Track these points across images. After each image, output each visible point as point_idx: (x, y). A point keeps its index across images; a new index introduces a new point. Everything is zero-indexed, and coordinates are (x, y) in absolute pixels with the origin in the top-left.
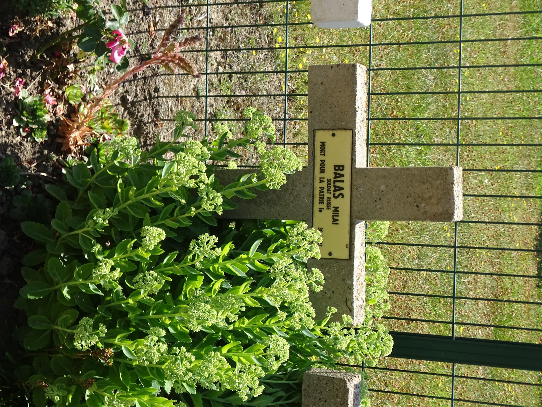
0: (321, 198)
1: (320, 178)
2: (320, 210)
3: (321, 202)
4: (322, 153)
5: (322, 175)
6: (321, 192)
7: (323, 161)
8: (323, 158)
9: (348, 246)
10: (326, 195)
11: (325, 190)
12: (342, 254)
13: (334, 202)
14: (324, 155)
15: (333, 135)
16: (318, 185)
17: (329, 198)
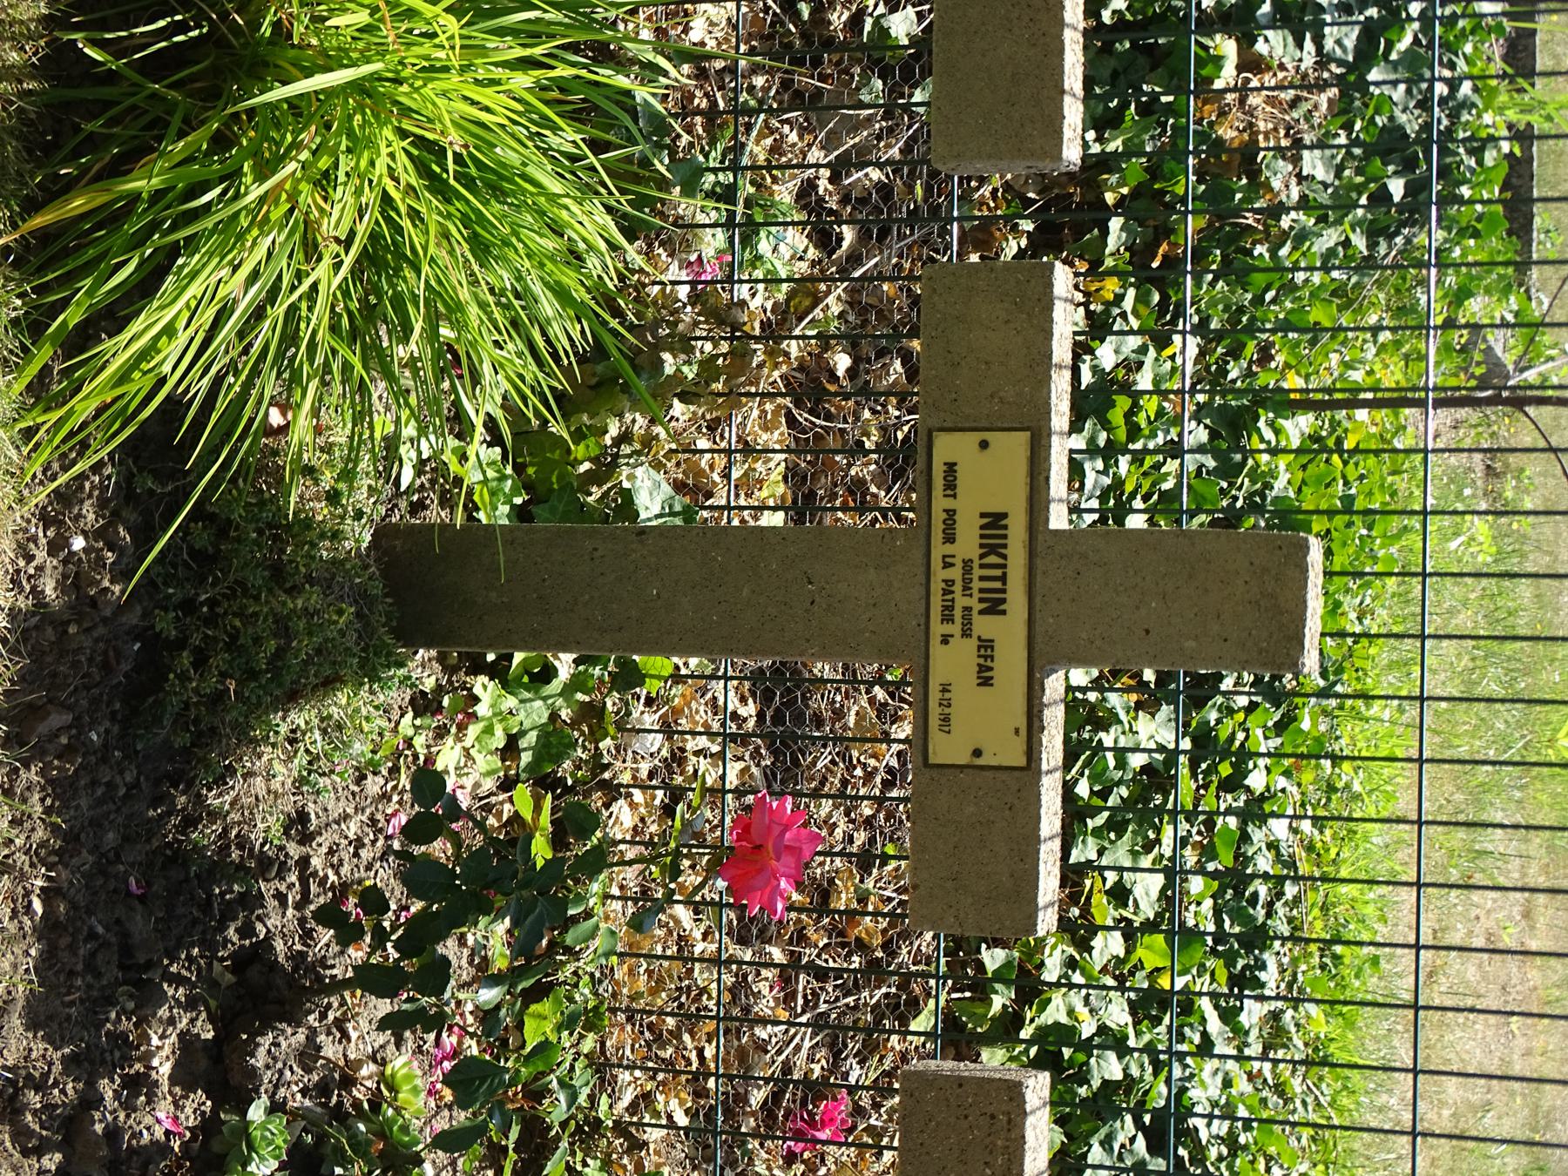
0: (945, 608)
2: (945, 640)
3: (948, 618)
5: (949, 549)
6: (946, 592)
7: (951, 513)
8: (949, 503)
9: (1023, 732)
10: (961, 601)
11: (958, 588)
13: (984, 626)
14: (954, 496)
16: (939, 574)
17: (968, 609)
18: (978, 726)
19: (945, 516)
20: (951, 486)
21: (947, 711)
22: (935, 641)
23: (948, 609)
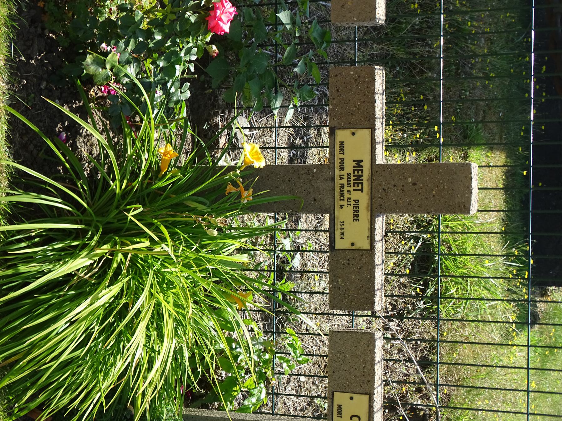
1: (340, 175)
5: (342, 173)
7: (342, 160)
8: (342, 156)
14: (343, 154)
15: (353, 134)
16: (338, 182)
18: (353, 235)
19: (340, 161)
20: (342, 150)
21: (343, 231)
23: (342, 195)
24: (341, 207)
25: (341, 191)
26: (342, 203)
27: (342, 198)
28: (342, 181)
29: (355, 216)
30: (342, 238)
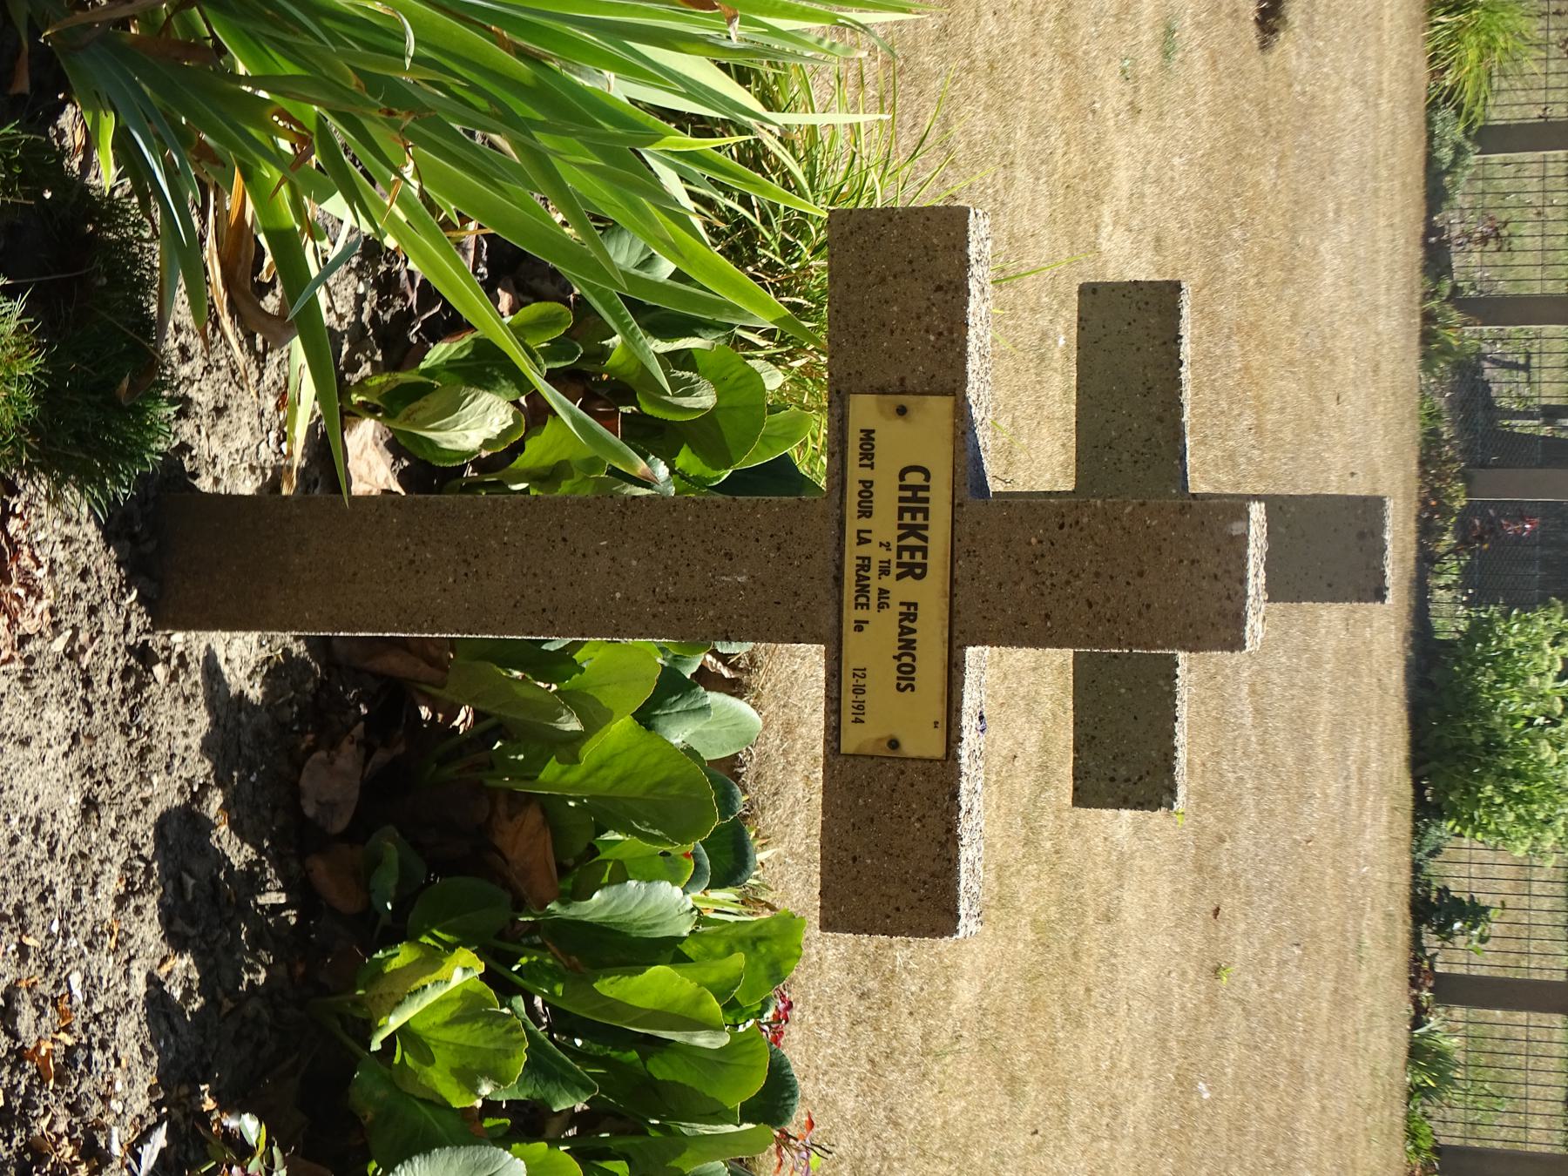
1: (859, 532)
4: (866, 462)
5: (864, 523)
7: (867, 485)
8: (866, 474)
12: (923, 743)
14: (872, 466)
16: (852, 552)
20: (867, 455)
21: (861, 698)
22: (848, 626)
23: (863, 590)
24: (859, 626)
25: (860, 578)
26: (861, 614)
27: (862, 600)
28: (864, 550)
29: (904, 630)
30: (857, 721)
